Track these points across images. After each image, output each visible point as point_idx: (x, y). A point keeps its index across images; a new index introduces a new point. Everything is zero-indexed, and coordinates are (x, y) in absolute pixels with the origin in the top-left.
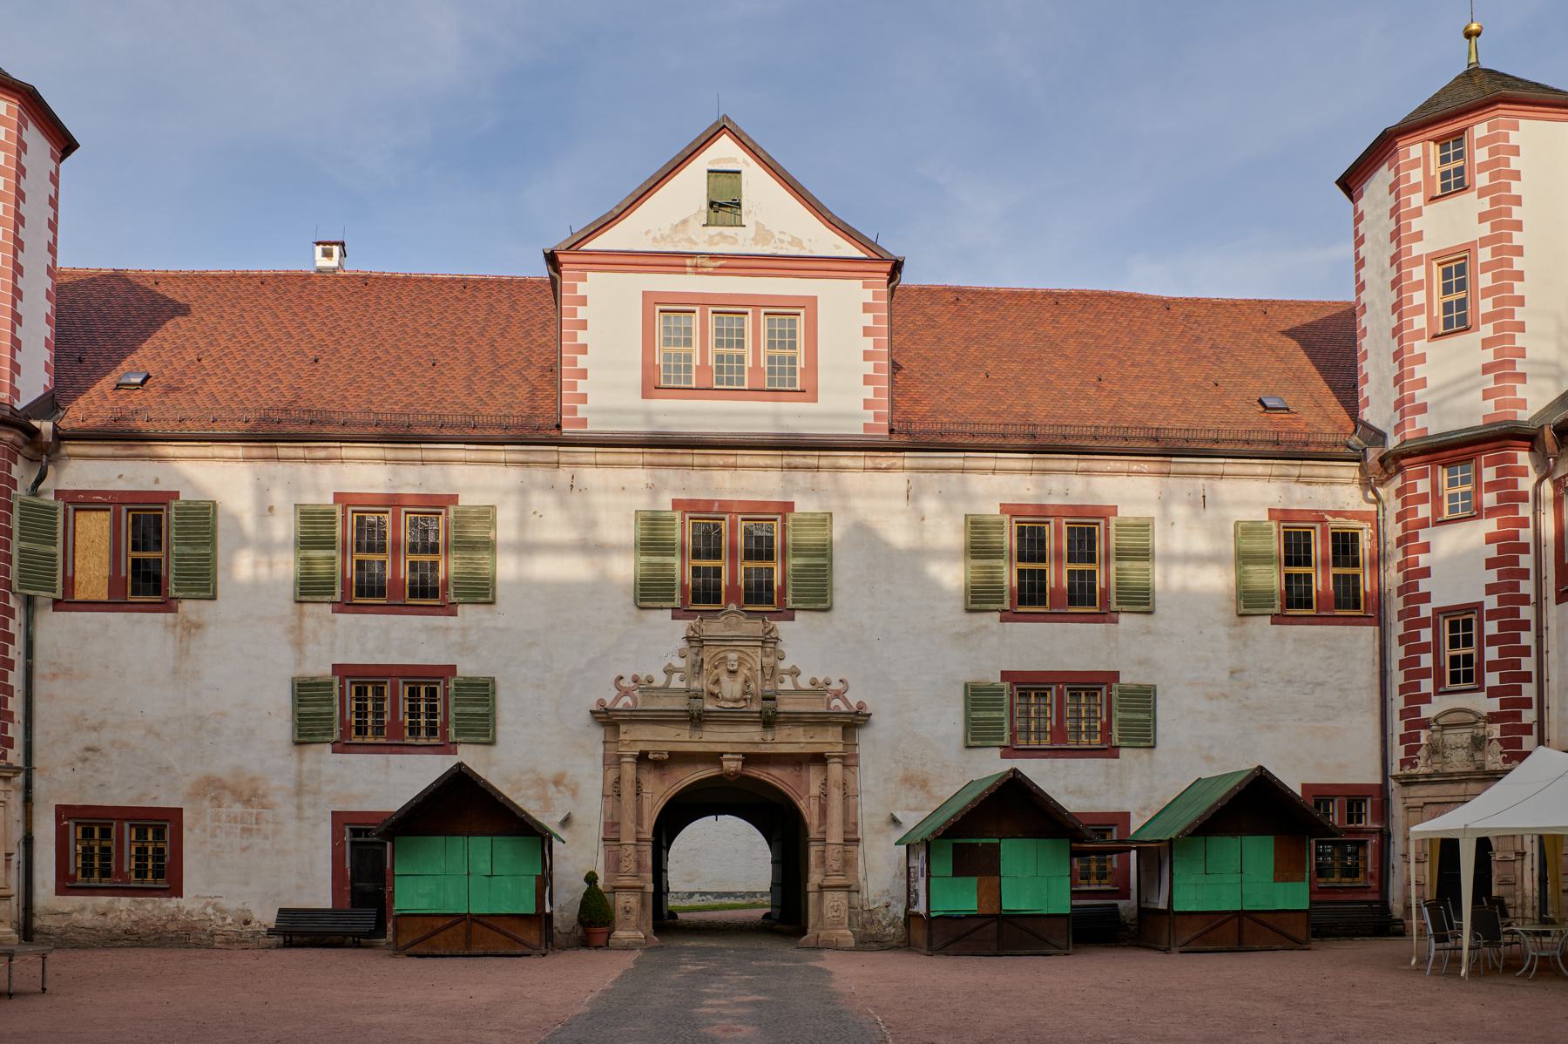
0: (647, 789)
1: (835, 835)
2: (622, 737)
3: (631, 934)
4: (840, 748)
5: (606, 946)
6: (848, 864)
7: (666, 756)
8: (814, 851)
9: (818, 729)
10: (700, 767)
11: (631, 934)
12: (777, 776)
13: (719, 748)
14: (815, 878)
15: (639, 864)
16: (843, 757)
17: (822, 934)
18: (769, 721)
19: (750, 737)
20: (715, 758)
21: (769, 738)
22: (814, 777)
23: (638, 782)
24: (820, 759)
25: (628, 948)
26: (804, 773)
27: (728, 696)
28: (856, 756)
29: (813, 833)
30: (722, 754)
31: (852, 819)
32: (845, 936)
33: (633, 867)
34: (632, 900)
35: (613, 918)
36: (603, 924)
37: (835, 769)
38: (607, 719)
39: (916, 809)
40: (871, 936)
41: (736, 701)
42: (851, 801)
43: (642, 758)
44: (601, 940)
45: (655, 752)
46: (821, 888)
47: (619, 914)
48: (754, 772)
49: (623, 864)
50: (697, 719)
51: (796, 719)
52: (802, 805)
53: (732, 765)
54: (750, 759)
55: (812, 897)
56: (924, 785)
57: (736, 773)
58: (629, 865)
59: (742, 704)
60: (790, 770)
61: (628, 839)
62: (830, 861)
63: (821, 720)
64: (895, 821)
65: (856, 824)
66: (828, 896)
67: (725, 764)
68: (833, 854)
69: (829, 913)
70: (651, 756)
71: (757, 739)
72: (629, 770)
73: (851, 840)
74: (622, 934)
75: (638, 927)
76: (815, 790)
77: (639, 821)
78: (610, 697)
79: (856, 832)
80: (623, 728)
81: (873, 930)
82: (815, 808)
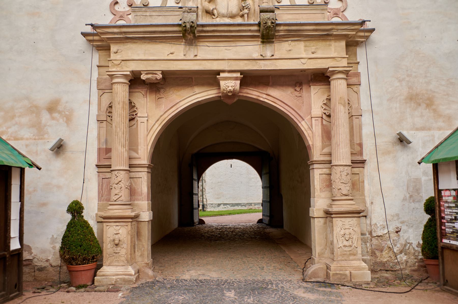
0: (141, 112)
1: (342, 156)
2: (113, 56)
3: (120, 270)
4: (344, 63)
5: (89, 285)
6: (356, 186)
7: (160, 76)
8: (317, 176)
9: (321, 44)
10: (197, 90)
11: (120, 270)
12: (277, 98)
13: (215, 66)
14: (319, 203)
15: (132, 192)
16: (347, 73)
17: (333, 266)
18: (268, 34)
19: (249, 54)
20: (211, 78)
21: (268, 54)
22: (315, 96)
23: (132, 105)
24: (322, 77)
25: (114, 289)
26: (304, 93)
27: (223, 10)
28: (358, 75)
29: (317, 154)
30: (218, 72)
31: (357, 141)
32: (359, 268)
33: (124, 195)
34: (122, 232)
35: (101, 251)
36: (85, 261)
37: (339, 85)
38: (101, 40)
39: (423, 129)
40: (383, 264)
41: (233, 17)
42: (355, 121)
43: (135, 81)
44: (84, 278)
45: (148, 72)
46: (328, 214)
47: (107, 248)
48: (254, 93)
49: (114, 192)
50: (190, 34)
51: (296, 33)
52: (303, 126)
53: (230, 84)
54: (249, 79)
55: (317, 226)
56: (430, 103)
57: (234, 94)
58: (120, 192)
59: (239, 20)
60: (290, 91)
61: (119, 161)
62: (337, 184)
63: (324, 33)
64: (402, 140)
65: (361, 145)
66: (338, 222)
67: (222, 83)
68: (341, 176)
69: (340, 243)
70: (143, 77)
71: (256, 55)
72: (121, 91)
73: (358, 163)
74: (110, 271)
75: (131, 261)
76: (317, 109)
77: (132, 145)
78: (105, 19)
79: (361, 153)
80: (114, 48)
81: (385, 257)
82: (317, 129)
